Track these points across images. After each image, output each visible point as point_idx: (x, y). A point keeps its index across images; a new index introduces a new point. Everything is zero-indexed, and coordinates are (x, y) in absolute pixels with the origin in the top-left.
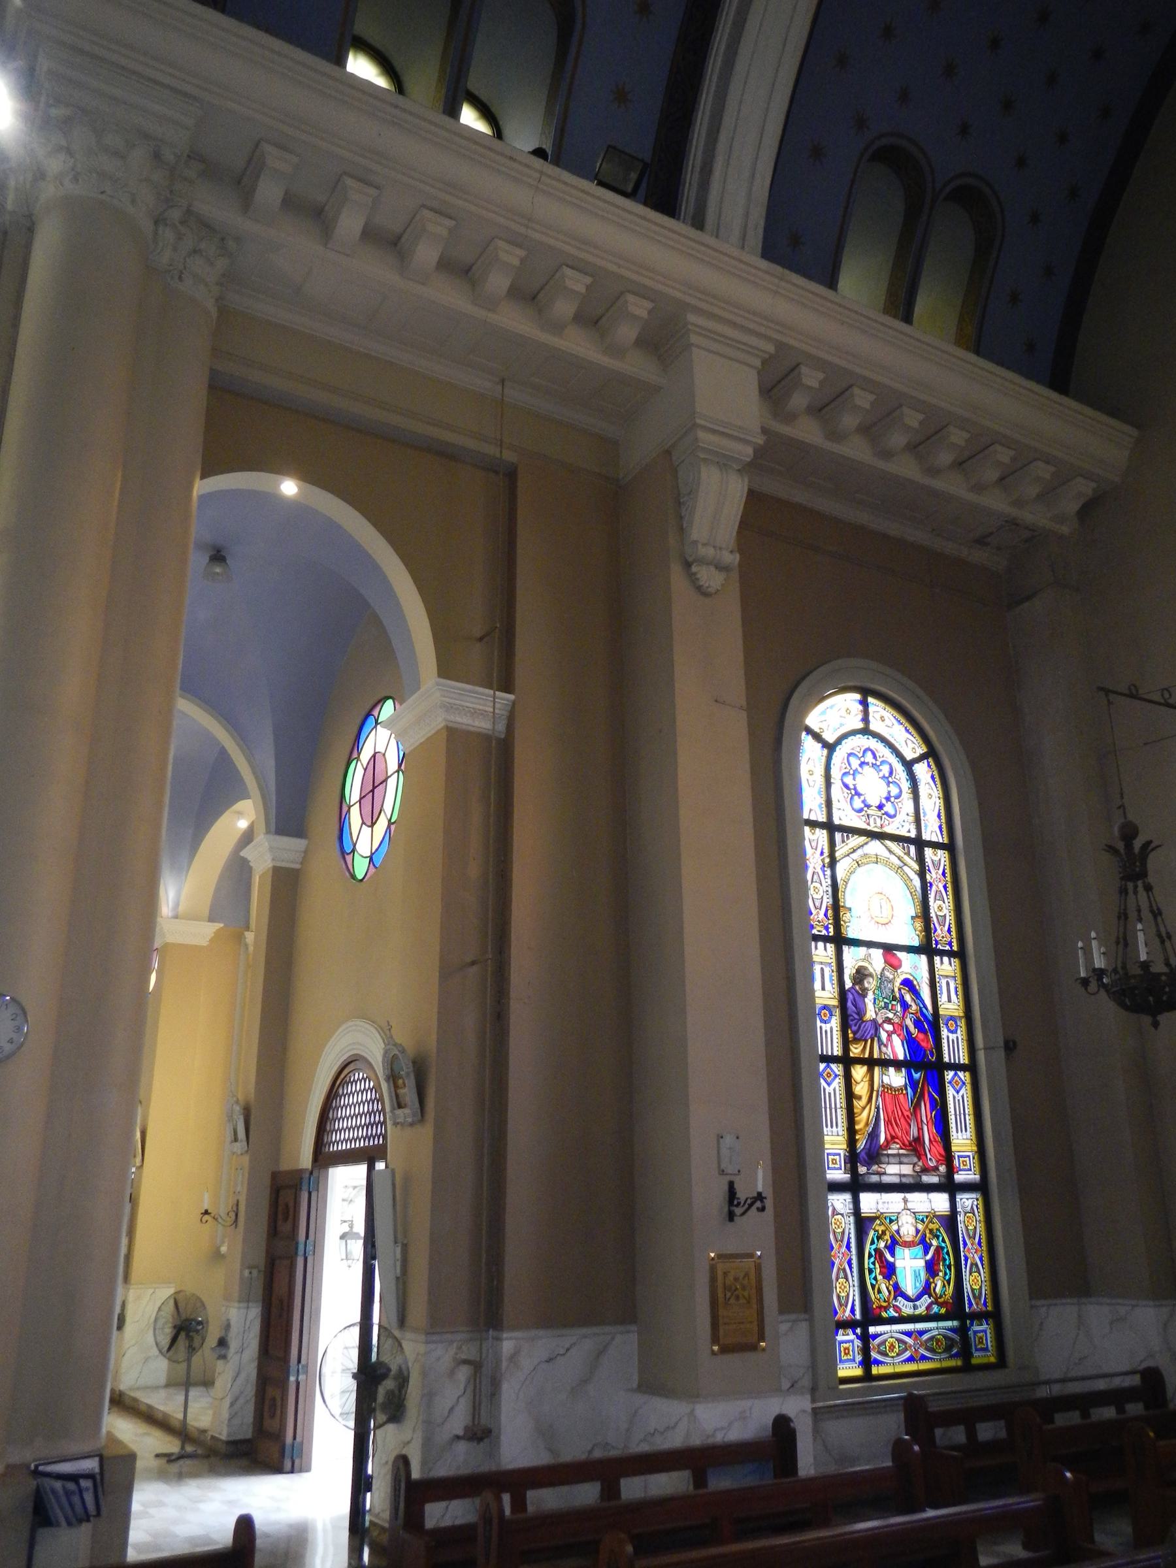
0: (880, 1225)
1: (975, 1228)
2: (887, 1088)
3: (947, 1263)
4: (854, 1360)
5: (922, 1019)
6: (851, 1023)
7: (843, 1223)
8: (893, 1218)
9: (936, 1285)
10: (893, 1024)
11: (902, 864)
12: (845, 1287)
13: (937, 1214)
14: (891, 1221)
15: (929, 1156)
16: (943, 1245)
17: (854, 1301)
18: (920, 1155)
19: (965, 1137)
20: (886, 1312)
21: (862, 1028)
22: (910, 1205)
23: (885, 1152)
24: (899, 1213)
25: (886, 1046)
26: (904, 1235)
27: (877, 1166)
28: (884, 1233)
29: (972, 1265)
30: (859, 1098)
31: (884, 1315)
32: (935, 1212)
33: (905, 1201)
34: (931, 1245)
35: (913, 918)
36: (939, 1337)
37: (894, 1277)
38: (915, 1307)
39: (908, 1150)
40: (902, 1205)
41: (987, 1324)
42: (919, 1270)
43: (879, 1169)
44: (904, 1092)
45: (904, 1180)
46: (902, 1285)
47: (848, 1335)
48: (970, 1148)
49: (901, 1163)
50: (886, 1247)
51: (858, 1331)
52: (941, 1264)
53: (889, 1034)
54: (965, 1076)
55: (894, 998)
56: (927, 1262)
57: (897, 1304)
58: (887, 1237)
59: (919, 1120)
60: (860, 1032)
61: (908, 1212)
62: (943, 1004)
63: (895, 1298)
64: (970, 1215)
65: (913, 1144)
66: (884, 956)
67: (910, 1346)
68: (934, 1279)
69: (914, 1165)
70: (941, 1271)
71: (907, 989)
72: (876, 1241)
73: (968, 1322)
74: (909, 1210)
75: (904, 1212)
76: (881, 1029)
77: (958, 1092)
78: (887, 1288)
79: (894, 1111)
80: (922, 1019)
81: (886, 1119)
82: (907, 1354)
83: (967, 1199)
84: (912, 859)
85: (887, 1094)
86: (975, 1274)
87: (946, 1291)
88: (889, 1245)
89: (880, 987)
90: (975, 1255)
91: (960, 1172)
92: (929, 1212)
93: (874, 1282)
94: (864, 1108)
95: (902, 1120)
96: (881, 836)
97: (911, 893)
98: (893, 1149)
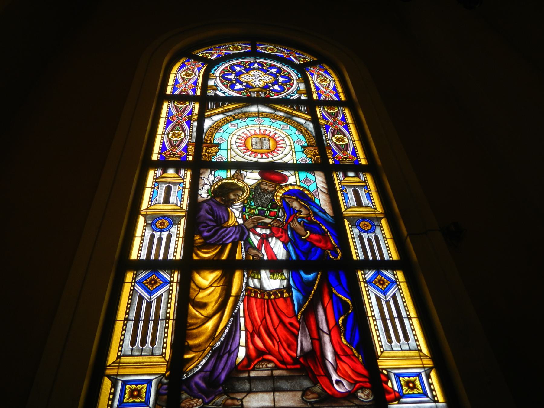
2: (255, 293)
5: (318, 222)
6: (202, 229)
10: (270, 228)
11: (289, 116)
15: (335, 377)
19: (407, 347)
21: (219, 234)
23: (246, 375)
25: (259, 249)
27: (225, 396)
30: (203, 305)
35: (303, 147)
39: (286, 369)
43: (230, 401)
44: (286, 295)
49: (275, 390)
53: (264, 239)
54: (394, 275)
55: (275, 206)
59: (314, 328)
60: (216, 237)
62: (350, 208)
65: (301, 360)
66: (260, 174)
69: (305, 392)
71: (294, 197)
76: (251, 234)
77: (385, 293)
79: (265, 318)
80: (318, 222)
81: (251, 330)
84: (304, 113)
85: (253, 300)
89: (254, 198)
91: (403, 400)
94: (208, 318)
95: (281, 332)
96: (266, 102)
97: (301, 132)
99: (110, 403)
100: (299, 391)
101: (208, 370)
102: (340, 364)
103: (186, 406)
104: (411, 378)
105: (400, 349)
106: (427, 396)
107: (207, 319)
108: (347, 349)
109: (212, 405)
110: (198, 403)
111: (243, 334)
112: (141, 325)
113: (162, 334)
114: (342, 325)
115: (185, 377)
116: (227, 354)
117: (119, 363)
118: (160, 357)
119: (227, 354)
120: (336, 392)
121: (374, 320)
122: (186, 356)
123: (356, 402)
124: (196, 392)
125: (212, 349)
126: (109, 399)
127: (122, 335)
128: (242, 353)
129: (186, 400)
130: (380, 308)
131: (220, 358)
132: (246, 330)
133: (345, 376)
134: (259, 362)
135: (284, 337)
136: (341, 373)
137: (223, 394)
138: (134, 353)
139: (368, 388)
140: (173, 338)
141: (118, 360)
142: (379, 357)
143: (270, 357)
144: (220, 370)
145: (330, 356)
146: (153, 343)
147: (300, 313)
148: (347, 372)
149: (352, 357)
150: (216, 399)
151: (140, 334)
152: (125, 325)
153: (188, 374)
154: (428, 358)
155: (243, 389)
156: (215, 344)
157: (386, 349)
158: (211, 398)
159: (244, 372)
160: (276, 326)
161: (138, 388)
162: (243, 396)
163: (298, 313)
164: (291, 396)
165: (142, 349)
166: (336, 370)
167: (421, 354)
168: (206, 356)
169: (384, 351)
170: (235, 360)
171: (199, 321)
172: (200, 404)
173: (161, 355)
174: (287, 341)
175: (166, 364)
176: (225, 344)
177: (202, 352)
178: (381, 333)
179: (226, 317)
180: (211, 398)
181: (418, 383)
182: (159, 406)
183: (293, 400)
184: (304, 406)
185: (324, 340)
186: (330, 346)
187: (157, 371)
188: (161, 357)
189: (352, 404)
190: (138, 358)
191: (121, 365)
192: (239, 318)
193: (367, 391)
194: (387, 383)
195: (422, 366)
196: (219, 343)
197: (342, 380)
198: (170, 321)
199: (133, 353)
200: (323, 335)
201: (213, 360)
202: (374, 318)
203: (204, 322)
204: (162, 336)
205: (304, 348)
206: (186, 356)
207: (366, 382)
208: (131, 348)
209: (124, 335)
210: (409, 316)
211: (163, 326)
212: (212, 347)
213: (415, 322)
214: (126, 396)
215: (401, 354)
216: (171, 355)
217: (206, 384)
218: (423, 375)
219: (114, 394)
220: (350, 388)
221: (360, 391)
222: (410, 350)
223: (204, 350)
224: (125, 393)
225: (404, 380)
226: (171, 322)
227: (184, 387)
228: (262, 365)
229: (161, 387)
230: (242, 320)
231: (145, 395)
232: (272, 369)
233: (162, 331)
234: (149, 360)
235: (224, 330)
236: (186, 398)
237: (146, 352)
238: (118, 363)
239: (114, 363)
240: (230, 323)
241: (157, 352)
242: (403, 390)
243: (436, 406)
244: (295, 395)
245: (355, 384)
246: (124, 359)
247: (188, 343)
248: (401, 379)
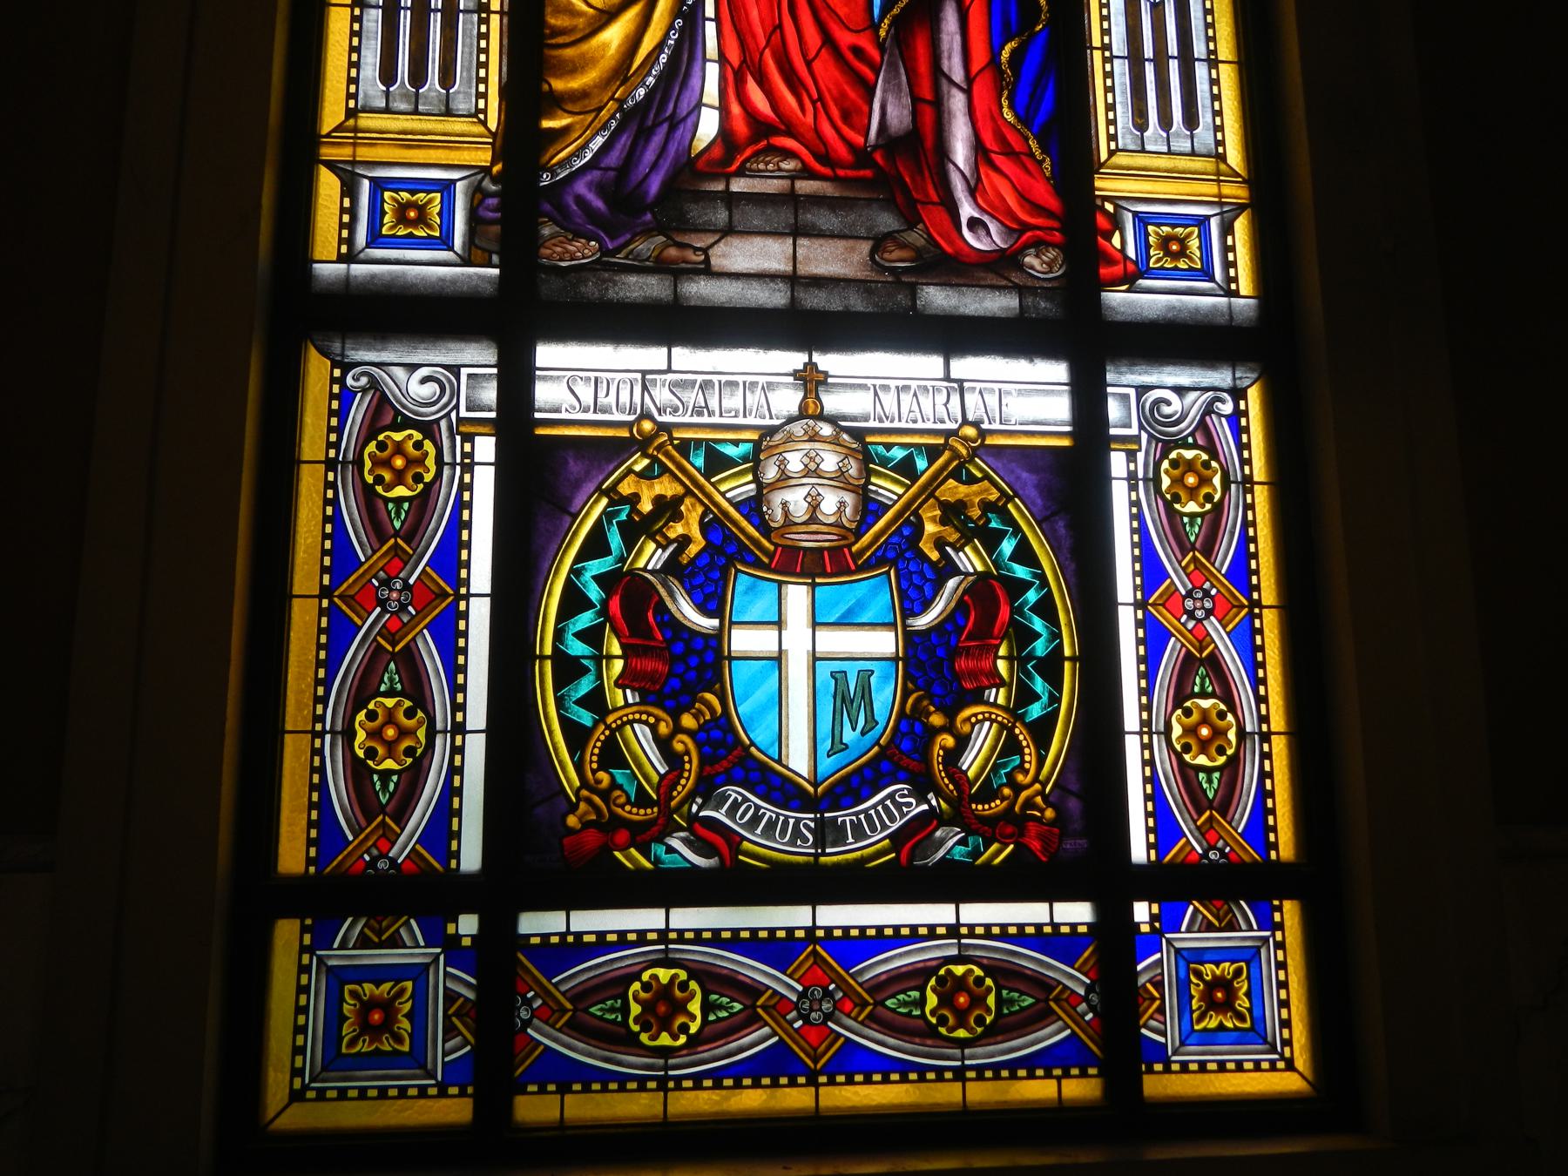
0: (646, 475)
1: (1218, 508)
3: (1040, 648)
4: (417, 1059)
7: (430, 462)
8: (731, 451)
9: (963, 742)
12: (403, 733)
13: (989, 441)
14: (717, 463)
15: (967, 210)
16: (1021, 572)
17: (451, 791)
18: (914, 204)
19: (1185, 145)
20: (646, 853)
22: (833, 402)
23: (720, 187)
24: (770, 431)
26: (789, 522)
27: (662, 239)
28: (668, 509)
29: (1188, 664)
31: (632, 858)
32: (983, 434)
33: (811, 381)
34: (953, 570)
36: (959, 970)
37: (709, 696)
38: (826, 833)
40: (788, 401)
41: (1266, 922)
42: (865, 677)
43: (673, 252)
45: (815, 300)
46: (761, 735)
47: (396, 942)
48: (1211, 189)
49: (797, 232)
50: (671, 567)
51: (468, 925)
52: (1002, 651)
56: (912, 639)
57: (720, 816)
58: (689, 525)
59: (923, 67)
61: (826, 430)
63: (707, 789)
64: (1189, 454)
65: (878, 157)
67: (779, 1005)
68: (951, 714)
69: (880, 243)
70: (1000, 683)
72: (615, 540)
73: (1141, 912)
74: (832, 420)
75: (798, 429)
78: (663, 744)
79: (780, 26)
81: (734, 57)
82: (755, 1041)
83: (1180, 391)
86: (1206, 704)
87: (1021, 768)
88: (692, 561)
90: (1213, 626)
92: (949, 434)
93: (586, 718)
95: (826, 69)
98: (756, 174)
99: (345, 233)
100: (867, 238)
101: (613, 165)
102: (987, 176)
103: (555, 255)
104: (1179, 230)
105: (1165, 149)
106: (1212, 279)
107: (604, 18)
108: (1011, 138)
109: (626, 258)
110: (586, 251)
111: (712, 71)
112: (405, 23)
113: (471, 53)
114: (1010, 67)
115: (546, 179)
116: (665, 126)
117: (356, 130)
118: (470, 119)
119: (665, 126)
120: (966, 248)
121: (1105, 60)
122: (546, 124)
123: (1016, 278)
124: (579, 221)
125: (620, 109)
126: (342, 226)
127: (352, 49)
128: (708, 126)
129: (553, 241)
130: (1130, 23)
131: (644, 135)
132: (722, 59)
133: (997, 209)
134: (756, 154)
135: (832, 87)
136: (985, 201)
137: (655, 233)
138: (395, 105)
139: (1054, 246)
140: (505, 69)
141: (351, 122)
142: (1102, 165)
143: (790, 143)
144: (644, 168)
145: (961, 152)
146: (447, 77)
147: (886, 21)
148: (1004, 200)
149: (1023, 157)
150: (637, 243)
151: (404, 49)
152: (358, 19)
153: (554, 174)
154: (1240, 179)
155: (709, 222)
156: (630, 93)
157: (1125, 145)
158: (622, 240)
159: (715, 177)
160: (812, 54)
161: (417, 201)
162: (711, 240)
163: (881, 19)
164: (841, 250)
165: (417, 94)
166: (973, 192)
167: (1223, 167)
168: (604, 127)
169: (1118, 150)
170: (687, 143)
171: (581, 21)
172: (593, 255)
173: (475, 115)
174: (841, 100)
175: (491, 140)
176: (658, 96)
177: (593, 115)
178: (1118, 99)
179: (662, 15)
180: (622, 240)
181: (1194, 244)
182: (479, 252)
183: (845, 260)
184: (873, 276)
185: (949, 108)
186: (965, 124)
187: (467, 158)
188: (475, 120)
189: (1004, 283)
190: (407, 120)
191: (360, 135)
192: (701, 22)
193: (1052, 254)
194: (1108, 236)
195: (1216, 199)
196: (642, 92)
197: (986, 219)
198: (492, 16)
199: (391, 105)
200: (949, 92)
201: (624, 141)
202: (1107, 54)
203: (596, 25)
204: (471, 62)
205: (888, 123)
206: (546, 124)
207: (1053, 229)
208: (384, 88)
209: (357, 50)
210: (1212, 57)
211: (471, 30)
212: (621, 101)
213: (1228, 75)
214: (387, 219)
215: (1164, 162)
216: (502, 117)
217: (605, 202)
218: (1214, 224)
219: (353, 212)
220: (1004, 240)
221: (1032, 251)
222: (1193, 153)
223: (600, 109)
224: (384, 213)
225: (1157, 234)
226: (495, 20)
227: (547, 207)
228: (767, 164)
229: (482, 201)
230: (710, 29)
231: (438, 221)
232: (793, 177)
233: (472, 44)
234: (440, 127)
235: (655, 55)
236: (552, 237)
237: (430, 104)
238: (349, 129)
239: (339, 128)
240: (674, 36)
241: (461, 105)
242: (1149, 257)
243: (1230, 303)
244: (853, 249)
245: (1021, 233)
246: (365, 121)
247: (550, 85)
248: (1151, 228)
